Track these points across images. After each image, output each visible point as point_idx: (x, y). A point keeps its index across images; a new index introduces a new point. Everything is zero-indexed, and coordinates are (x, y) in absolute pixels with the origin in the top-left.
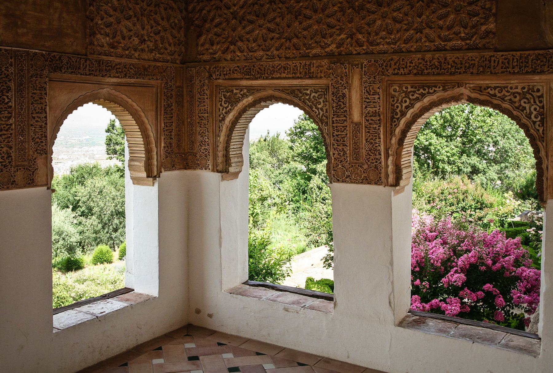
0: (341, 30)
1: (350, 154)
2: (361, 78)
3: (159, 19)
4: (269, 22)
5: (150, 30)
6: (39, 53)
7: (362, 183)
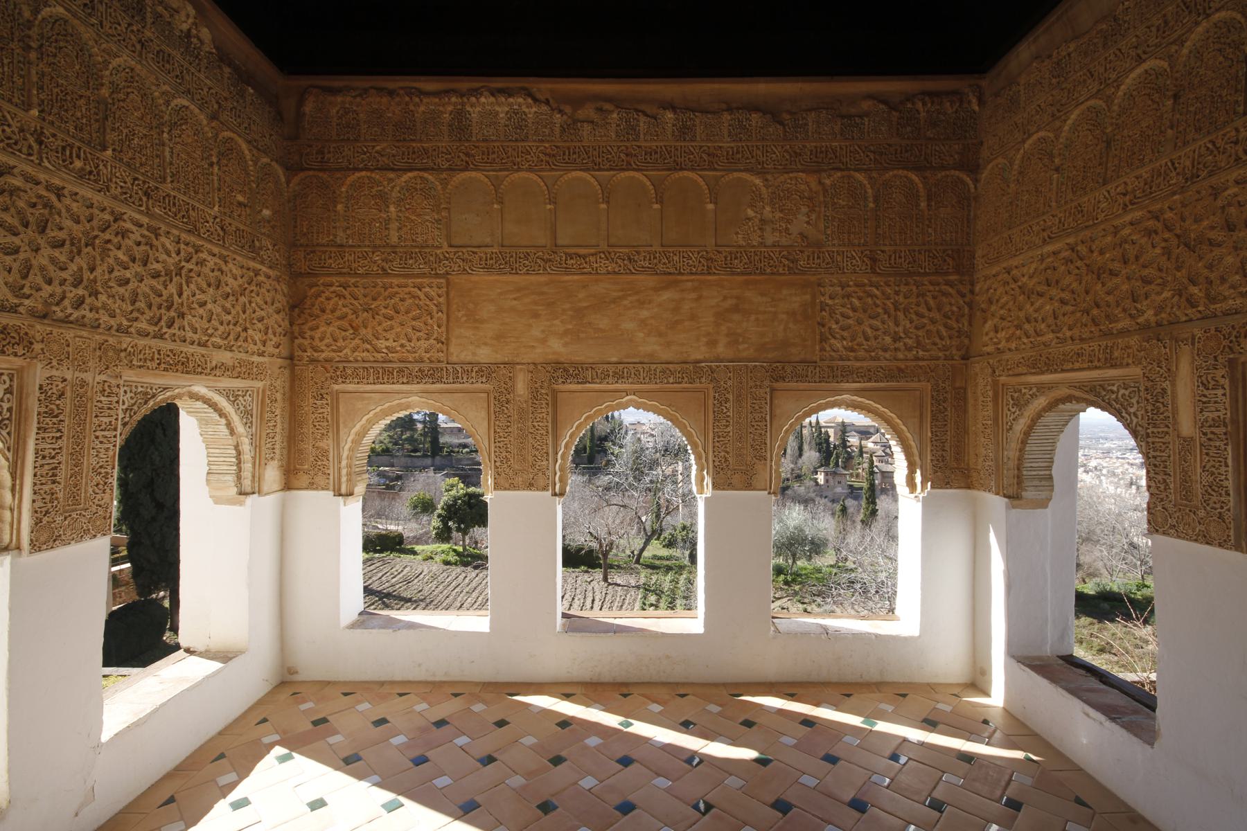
0: (1164, 285)
1: (1175, 489)
2: (1193, 362)
4: (1063, 290)
5: (908, 325)
7: (1196, 540)
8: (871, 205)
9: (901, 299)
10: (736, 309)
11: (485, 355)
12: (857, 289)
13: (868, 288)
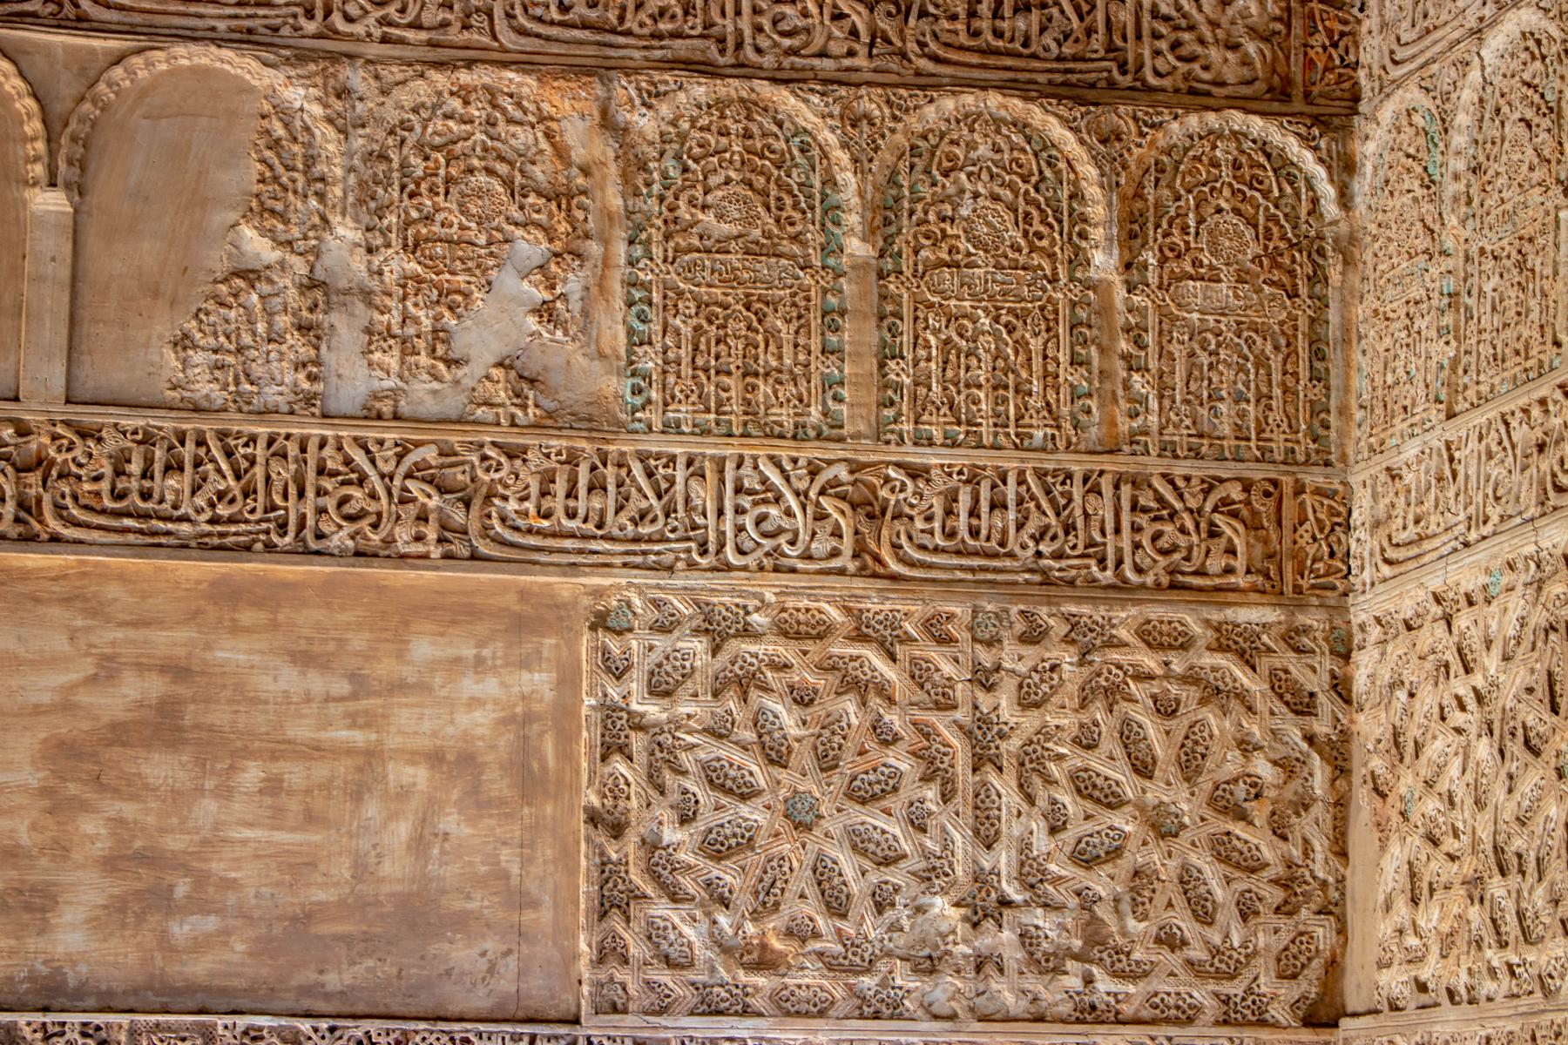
3: (1120, 775)
5: (1041, 843)
6: (271, 1029)
8: (857, 248)
9: (1004, 703)
10: (163, 726)
12: (785, 651)
13: (840, 648)
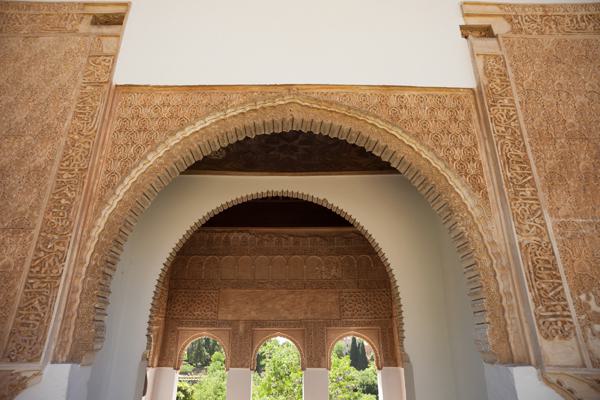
10: (313, 301)
11: (230, 317)
